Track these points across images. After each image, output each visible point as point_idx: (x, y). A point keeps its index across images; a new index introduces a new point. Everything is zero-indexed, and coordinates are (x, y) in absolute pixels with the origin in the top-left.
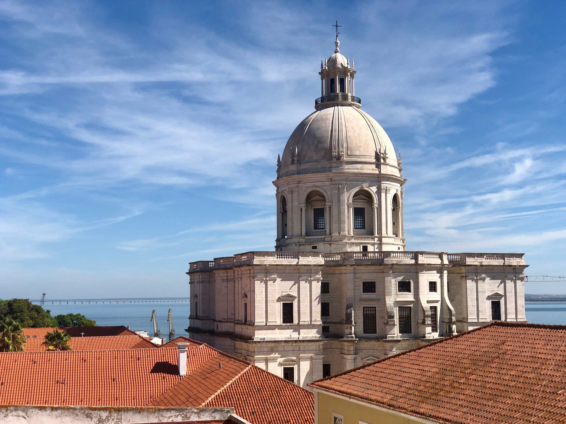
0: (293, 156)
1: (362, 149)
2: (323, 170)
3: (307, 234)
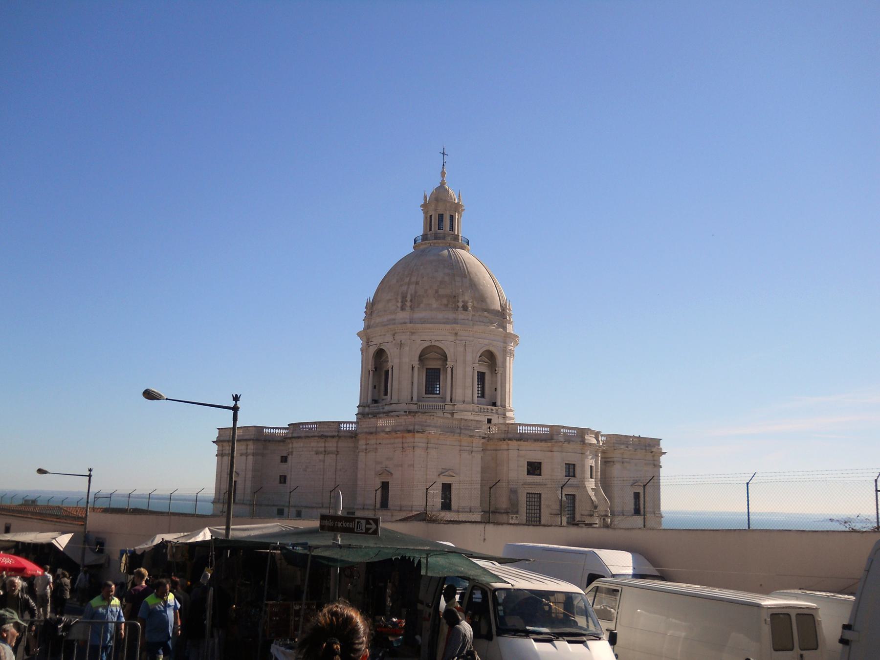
1: (488, 301)
2: (447, 322)
3: (419, 400)
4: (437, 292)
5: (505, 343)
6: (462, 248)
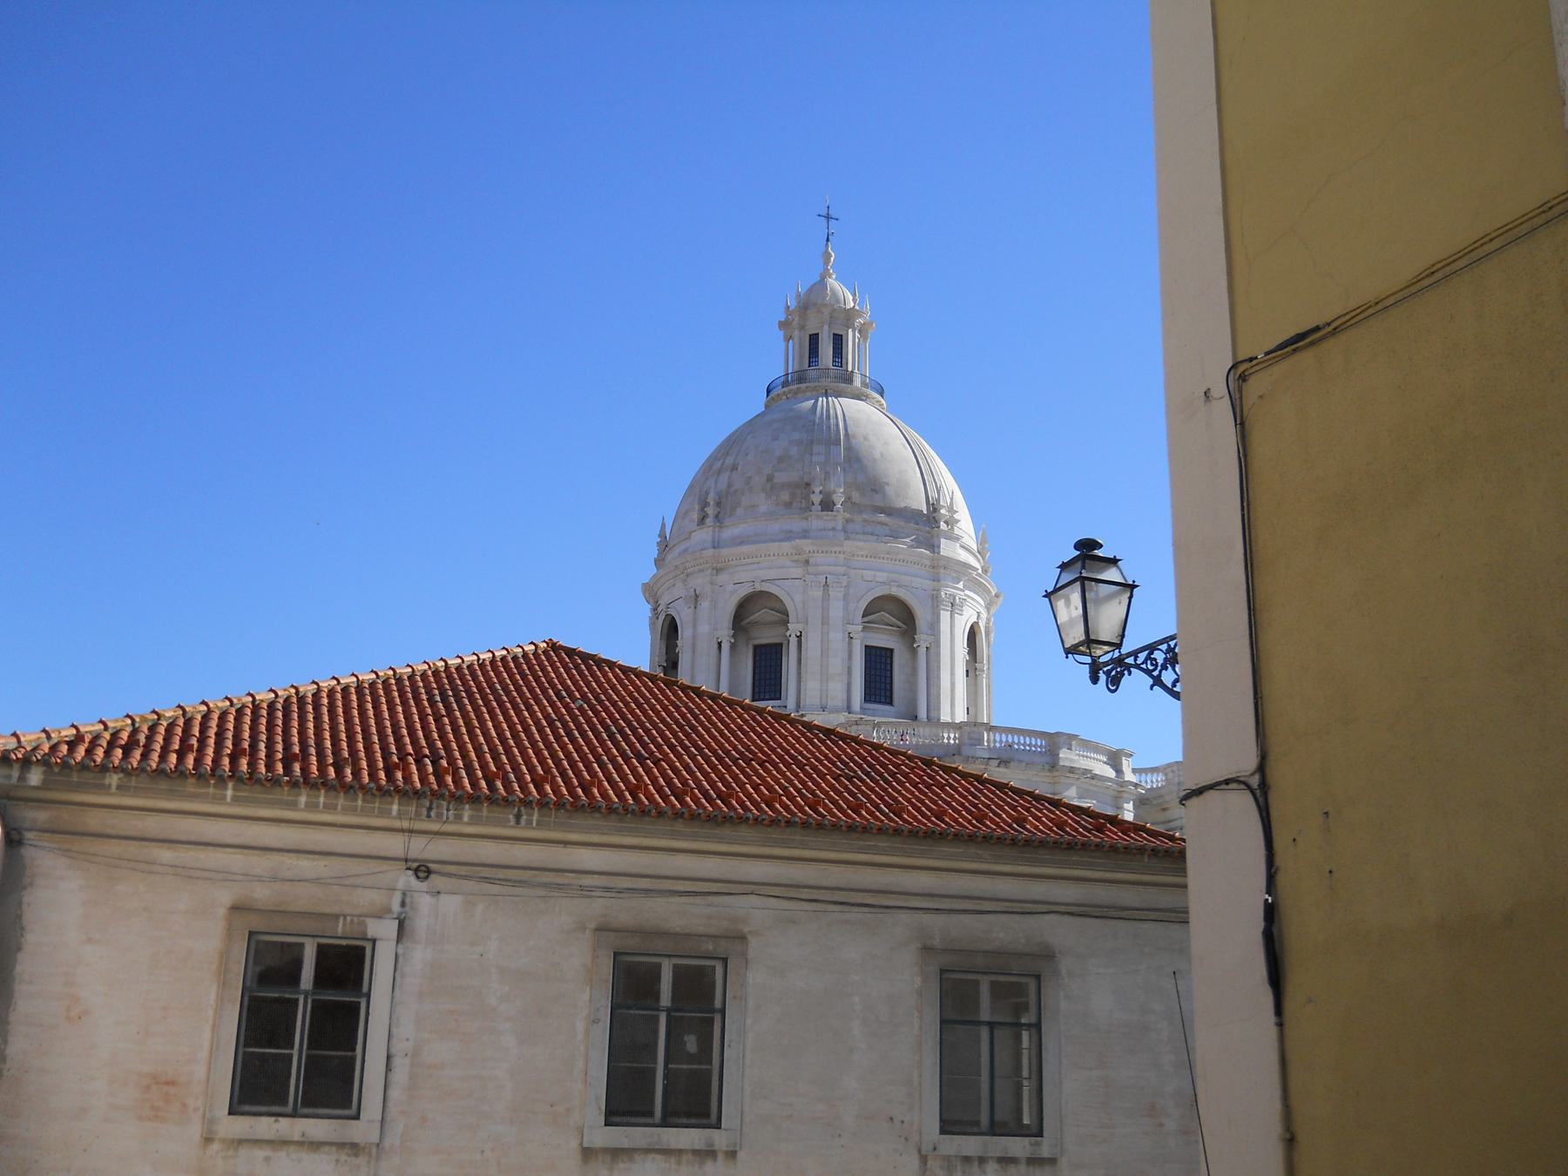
0: (705, 504)
1: (890, 491)
2: (789, 536)
4: (770, 479)
5: (936, 579)
6: (858, 396)
